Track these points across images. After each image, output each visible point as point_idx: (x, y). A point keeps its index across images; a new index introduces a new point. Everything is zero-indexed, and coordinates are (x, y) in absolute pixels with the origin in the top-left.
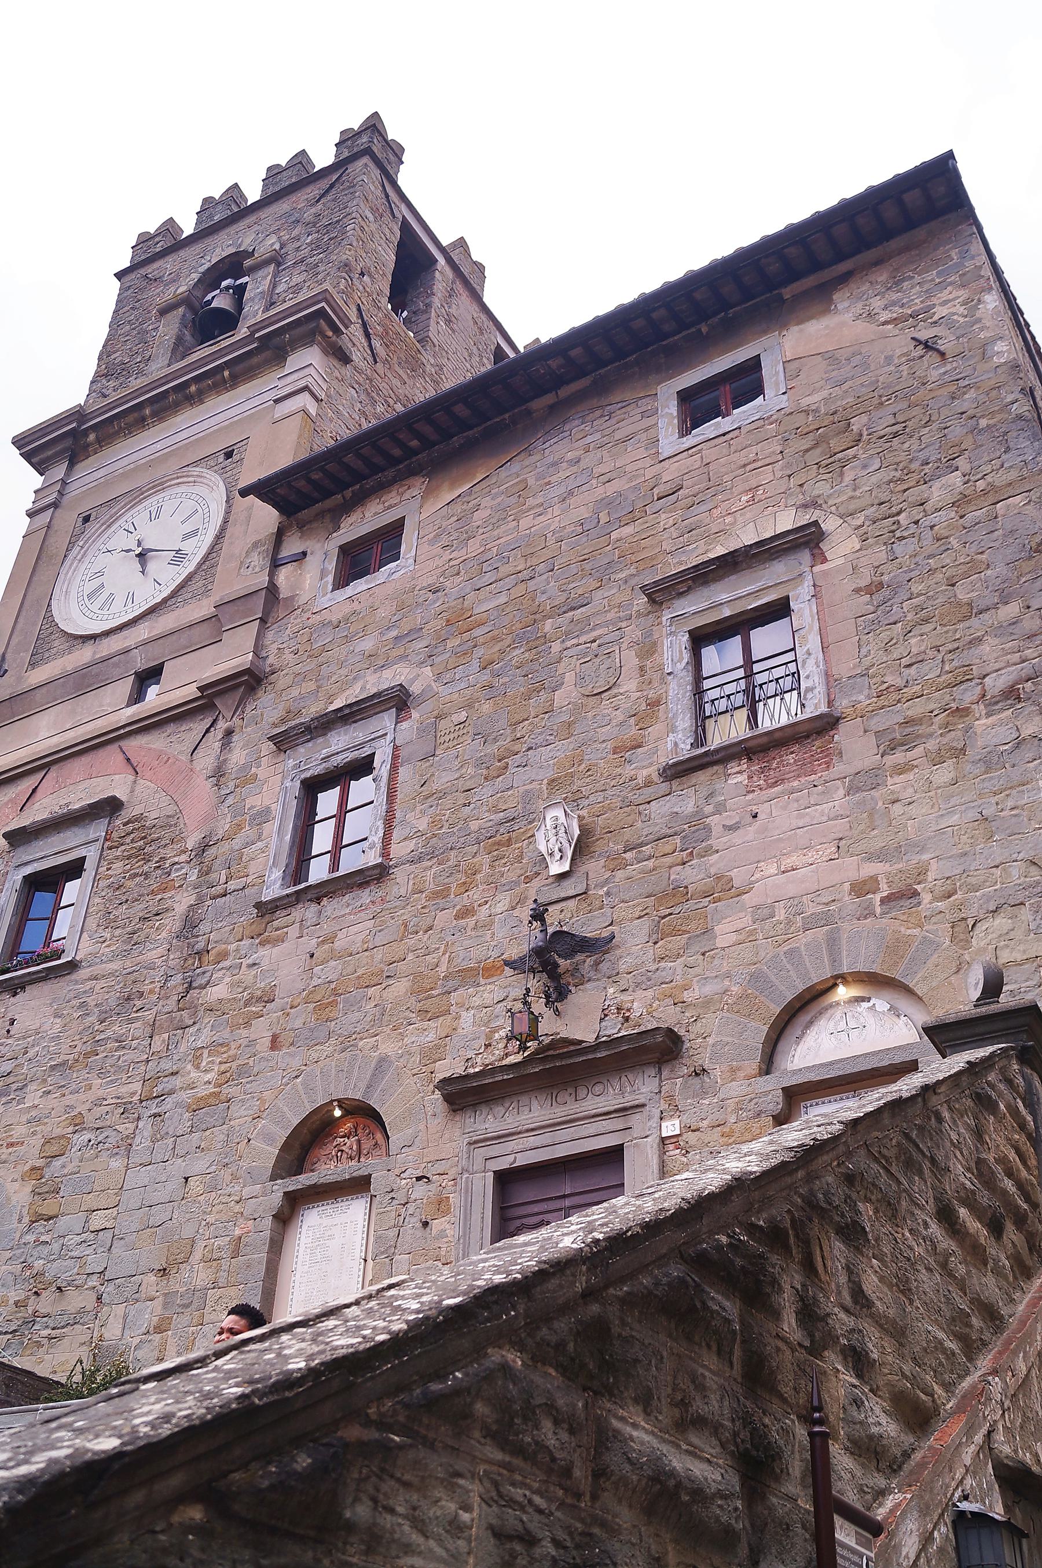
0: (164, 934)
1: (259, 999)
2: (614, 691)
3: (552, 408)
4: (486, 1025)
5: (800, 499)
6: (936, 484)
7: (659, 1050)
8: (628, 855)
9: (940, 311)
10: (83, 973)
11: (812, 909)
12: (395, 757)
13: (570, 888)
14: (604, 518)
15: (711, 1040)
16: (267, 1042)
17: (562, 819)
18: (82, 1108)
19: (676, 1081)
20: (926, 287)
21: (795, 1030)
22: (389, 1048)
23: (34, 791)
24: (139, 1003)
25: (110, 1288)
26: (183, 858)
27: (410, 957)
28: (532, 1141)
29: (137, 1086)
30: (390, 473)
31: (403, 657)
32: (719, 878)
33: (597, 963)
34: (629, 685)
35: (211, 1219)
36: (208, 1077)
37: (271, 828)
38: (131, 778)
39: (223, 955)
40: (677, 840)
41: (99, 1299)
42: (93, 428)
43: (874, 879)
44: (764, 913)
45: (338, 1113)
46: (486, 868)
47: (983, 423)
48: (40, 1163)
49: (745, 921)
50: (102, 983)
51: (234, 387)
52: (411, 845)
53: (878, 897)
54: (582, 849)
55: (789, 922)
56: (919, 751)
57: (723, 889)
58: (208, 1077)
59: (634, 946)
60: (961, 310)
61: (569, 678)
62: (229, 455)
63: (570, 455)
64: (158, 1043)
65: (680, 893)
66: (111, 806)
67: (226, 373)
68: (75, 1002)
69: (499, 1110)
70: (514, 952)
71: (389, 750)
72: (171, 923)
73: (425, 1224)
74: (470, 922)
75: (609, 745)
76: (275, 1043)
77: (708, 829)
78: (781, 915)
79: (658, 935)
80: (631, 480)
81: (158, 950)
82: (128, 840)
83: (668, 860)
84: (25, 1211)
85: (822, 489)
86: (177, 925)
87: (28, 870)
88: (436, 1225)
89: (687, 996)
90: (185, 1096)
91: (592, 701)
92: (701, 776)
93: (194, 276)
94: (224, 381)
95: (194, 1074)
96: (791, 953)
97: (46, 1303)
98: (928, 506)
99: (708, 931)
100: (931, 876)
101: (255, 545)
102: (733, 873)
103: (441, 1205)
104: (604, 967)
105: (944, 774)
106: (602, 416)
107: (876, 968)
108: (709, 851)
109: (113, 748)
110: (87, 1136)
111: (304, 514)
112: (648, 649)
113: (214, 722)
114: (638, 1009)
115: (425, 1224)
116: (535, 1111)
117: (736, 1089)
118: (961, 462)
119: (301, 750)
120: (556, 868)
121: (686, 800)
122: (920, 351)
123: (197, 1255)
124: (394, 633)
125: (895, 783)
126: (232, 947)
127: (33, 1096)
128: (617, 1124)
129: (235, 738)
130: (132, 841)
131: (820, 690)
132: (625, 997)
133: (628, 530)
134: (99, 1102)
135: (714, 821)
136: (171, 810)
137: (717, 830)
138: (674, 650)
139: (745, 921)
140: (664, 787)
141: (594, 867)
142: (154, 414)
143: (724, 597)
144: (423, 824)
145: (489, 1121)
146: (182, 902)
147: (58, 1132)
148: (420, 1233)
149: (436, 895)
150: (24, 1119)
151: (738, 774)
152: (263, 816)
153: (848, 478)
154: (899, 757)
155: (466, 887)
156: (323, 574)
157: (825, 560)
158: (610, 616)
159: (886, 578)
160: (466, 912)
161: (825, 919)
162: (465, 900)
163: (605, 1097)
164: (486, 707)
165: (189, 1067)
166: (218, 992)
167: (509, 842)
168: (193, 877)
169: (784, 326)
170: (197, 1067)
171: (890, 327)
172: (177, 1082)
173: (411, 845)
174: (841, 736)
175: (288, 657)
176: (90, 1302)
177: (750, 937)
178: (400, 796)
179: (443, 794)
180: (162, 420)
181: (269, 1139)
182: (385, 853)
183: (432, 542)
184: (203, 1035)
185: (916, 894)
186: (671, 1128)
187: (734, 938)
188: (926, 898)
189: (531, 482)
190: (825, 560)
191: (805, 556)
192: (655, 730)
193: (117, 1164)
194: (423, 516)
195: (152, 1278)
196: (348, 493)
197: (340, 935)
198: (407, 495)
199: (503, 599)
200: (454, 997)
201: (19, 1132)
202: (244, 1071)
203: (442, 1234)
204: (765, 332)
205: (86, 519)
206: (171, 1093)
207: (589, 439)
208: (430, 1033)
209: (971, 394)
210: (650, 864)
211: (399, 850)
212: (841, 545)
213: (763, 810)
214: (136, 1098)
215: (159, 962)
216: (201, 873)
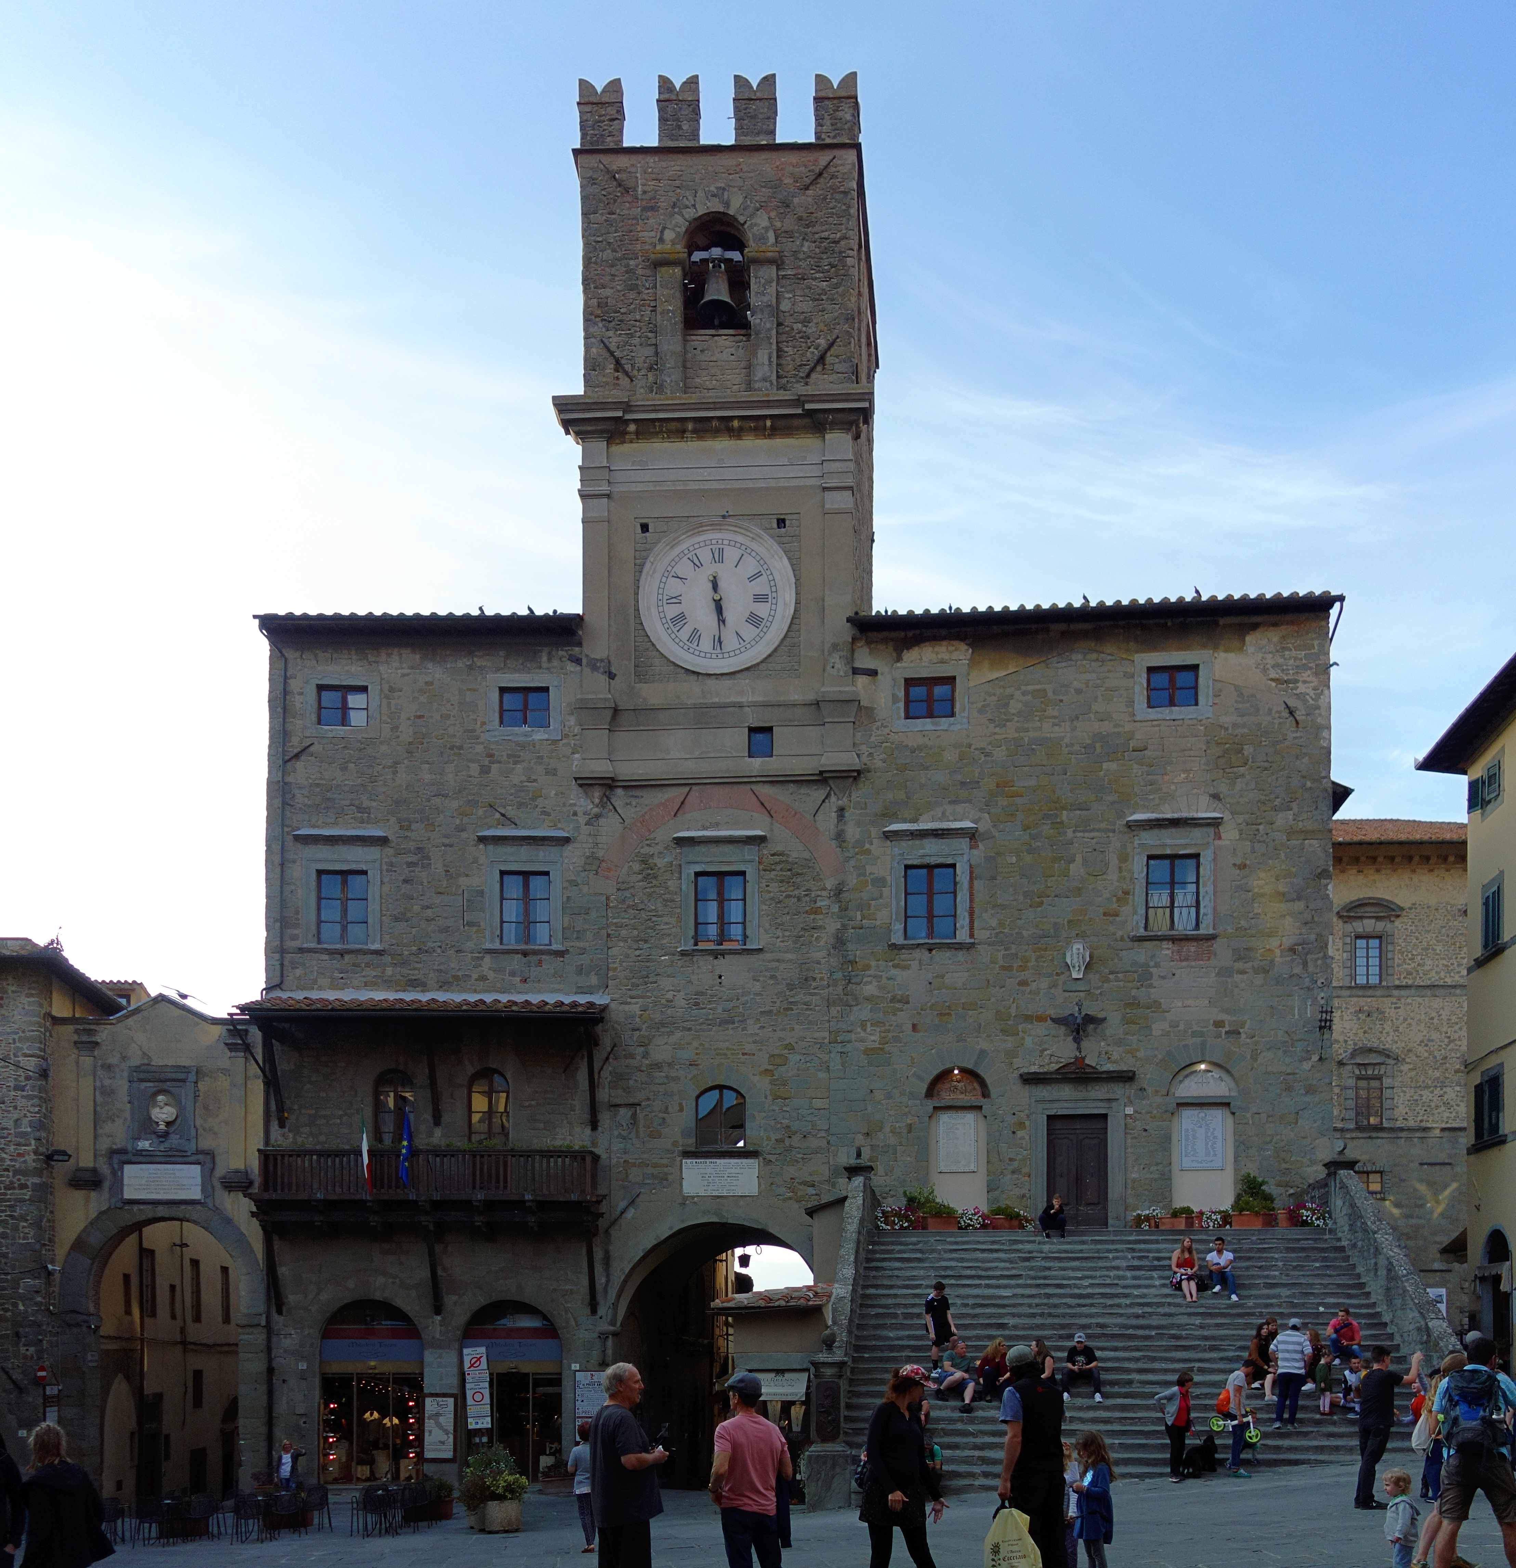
0: (822, 943)
1: (899, 1001)
2: (1105, 877)
3: (1063, 633)
4: (1040, 1045)
5: (1212, 791)
6: (1281, 815)
7: (1127, 1077)
8: (1111, 977)
9: (1301, 688)
10: (767, 956)
11: (1195, 1028)
12: (971, 873)
13: (1081, 986)
14: (1098, 750)
15: (1148, 1076)
16: (910, 1027)
17: (1082, 950)
18: (793, 1041)
19: (1130, 1090)
20: (1298, 663)
21: (1180, 1077)
22: (984, 1045)
23: (682, 803)
24: (814, 984)
25: (834, 1138)
26: (824, 893)
27: (993, 999)
28: (1066, 1105)
29: (827, 1034)
30: (944, 632)
31: (970, 801)
32: (1155, 1002)
33: (1095, 1029)
34: (1113, 875)
35: (892, 1113)
36: (873, 1038)
37: (886, 890)
38: (768, 819)
39: (868, 967)
40: (1136, 975)
41: (828, 1143)
42: (635, 421)
43: (1223, 1021)
44: (1174, 1025)
45: (956, 1072)
46: (1033, 963)
47: (1309, 784)
48: (770, 1067)
49: (1165, 1026)
50: (783, 966)
51: (771, 436)
52: (987, 934)
53: (1224, 1030)
54: (1088, 967)
55: (1185, 1031)
56: (1249, 965)
57: (1155, 1005)
58: (873, 1038)
59: (1114, 1026)
60: (1312, 693)
61: (1079, 858)
62: (781, 523)
63: (1076, 684)
64: (834, 1011)
65: (1135, 1004)
66: (762, 839)
67: (768, 423)
68: (768, 974)
69: (1049, 1088)
70: (1052, 1012)
71: (967, 868)
72: (826, 938)
73: (1014, 1133)
74: (1028, 989)
75: (1101, 910)
76: (915, 1027)
77: (1151, 974)
78: (1182, 1027)
79: (1126, 1021)
80: (1115, 726)
81: (819, 952)
82: (778, 868)
83: (1130, 985)
84: (768, 1093)
85: (1223, 788)
86: (832, 940)
87: (698, 868)
88: (1020, 1133)
89: (1138, 1054)
90: (861, 1046)
91: (1092, 878)
92: (1148, 944)
93: (678, 219)
94: (765, 428)
95: (863, 1034)
96: (1185, 1046)
97: (796, 1141)
98: (1274, 826)
99: (1149, 1027)
100: (1247, 1026)
101: (835, 647)
102: (1162, 1001)
103: (1021, 1125)
104: (1098, 1030)
105: (1259, 980)
106: (1097, 660)
107: (1219, 1062)
108: (1151, 986)
109: (748, 787)
110: (798, 1057)
111: (873, 635)
112: (1124, 858)
113: (828, 796)
114: (1115, 1056)
115: (1014, 1133)
116: (1066, 1092)
117: (1158, 1099)
118: (1294, 805)
119: (903, 844)
120: (1075, 975)
121: (1141, 954)
122: (1286, 714)
123: (887, 1129)
124: (959, 777)
125: (1237, 977)
126: (873, 963)
127: (752, 1028)
128: (1105, 1105)
129: (847, 814)
130: (781, 870)
131: (1210, 917)
132: (1110, 1048)
133: (1113, 766)
134: (802, 1039)
135: (1154, 970)
136: (807, 855)
137: (1155, 977)
138: (1138, 864)
139: (1165, 1026)
140: (1130, 944)
141: (1094, 977)
142: (695, 431)
143: (1168, 841)
144: (994, 923)
145: (1043, 1092)
146: (832, 926)
147: (777, 1052)
148: (1011, 1135)
149: (1003, 968)
150: (751, 1040)
151: (1167, 949)
152: (880, 882)
153: (1238, 787)
154: (1240, 965)
155: (1022, 968)
156: (895, 700)
157: (1220, 838)
158: (1103, 825)
159: (1248, 862)
160: (1024, 983)
161: (1201, 1034)
162: (1023, 976)
163: (1100, 1091)
164: (1028, 858)
165: (859, 1030)
166: (870, 989)
167: (1046, 950)
168: (835, 908)
169: (1216, 648)
170: (865, 1030)
171: (1274, 684)
172: (853, 1036)
173: (987, 934)
174: (1217, 945)
175: (880, 764)
176: (824, 1143)
177: (1167, 1034)
178: (976, 900)
179: (1004, 907)
180: (700, 438)
181: (921, 1079)
182: (972, 936)
183: (981, 711)
184: (863, 1012)
185: (1239, 1033)
186: (1129, 1110)
187: (1160, 1032)
188: (1243, 1036)
189: (1050, 694)
190: (1220, 838)
191: (1211, 830)
192: (1126, 910)
193: (822, 1075)
194: (971, 684)
195: (860, 1136)
196: (910, 634)
197: (947, 976)
198: (955, 655)
199: (1033, 782)
200: (1020, 1027)
201: (749, 1048)
202: (897, 1039)
203: (1022, 1138)
204: (1204, 646)
205: (645, 528)
206: (849, 1042)
207: (1088, 676)
208: (1010, 1043)
209: (1306, 760)
210: (1122, 984)
211: (981, 935)
212: (1229, 833)
213: (1178, 972)
214: (826, 1041)
215: (823, 961)
216: (841, 909)
